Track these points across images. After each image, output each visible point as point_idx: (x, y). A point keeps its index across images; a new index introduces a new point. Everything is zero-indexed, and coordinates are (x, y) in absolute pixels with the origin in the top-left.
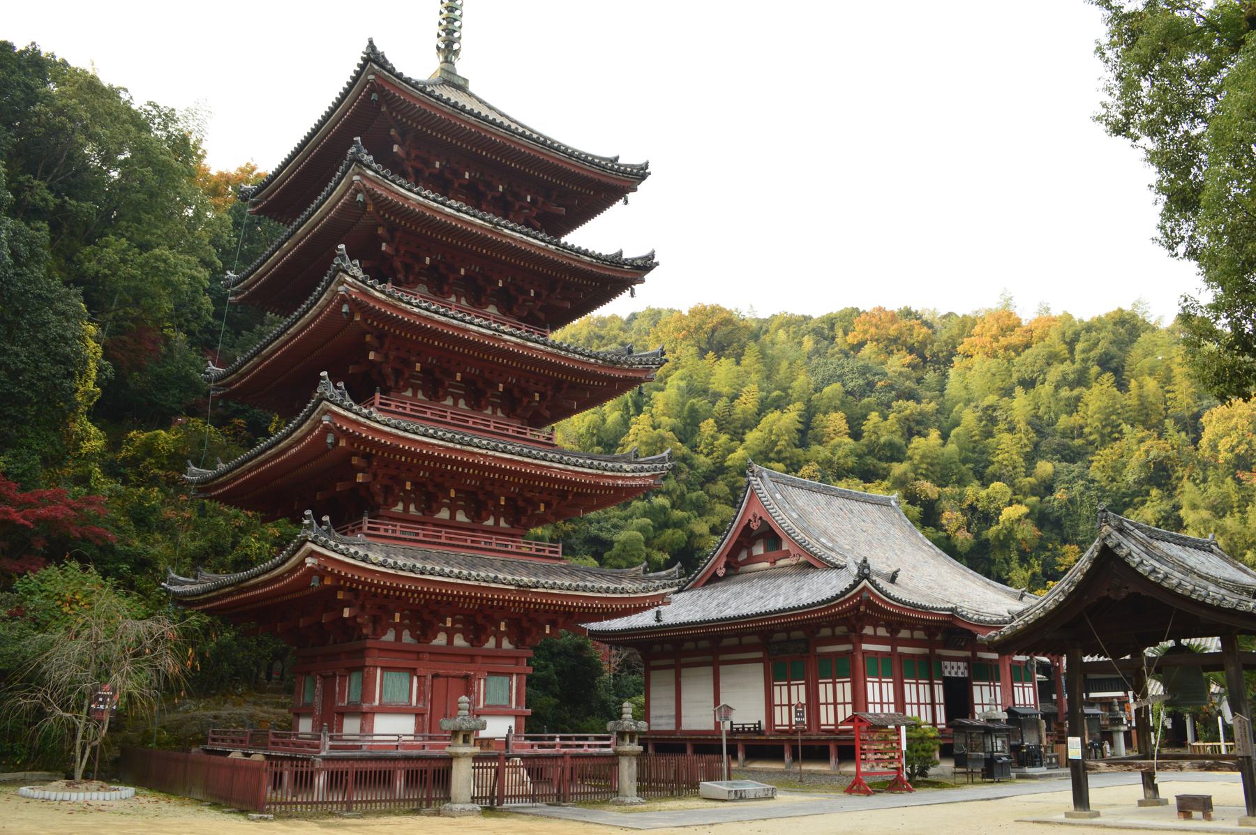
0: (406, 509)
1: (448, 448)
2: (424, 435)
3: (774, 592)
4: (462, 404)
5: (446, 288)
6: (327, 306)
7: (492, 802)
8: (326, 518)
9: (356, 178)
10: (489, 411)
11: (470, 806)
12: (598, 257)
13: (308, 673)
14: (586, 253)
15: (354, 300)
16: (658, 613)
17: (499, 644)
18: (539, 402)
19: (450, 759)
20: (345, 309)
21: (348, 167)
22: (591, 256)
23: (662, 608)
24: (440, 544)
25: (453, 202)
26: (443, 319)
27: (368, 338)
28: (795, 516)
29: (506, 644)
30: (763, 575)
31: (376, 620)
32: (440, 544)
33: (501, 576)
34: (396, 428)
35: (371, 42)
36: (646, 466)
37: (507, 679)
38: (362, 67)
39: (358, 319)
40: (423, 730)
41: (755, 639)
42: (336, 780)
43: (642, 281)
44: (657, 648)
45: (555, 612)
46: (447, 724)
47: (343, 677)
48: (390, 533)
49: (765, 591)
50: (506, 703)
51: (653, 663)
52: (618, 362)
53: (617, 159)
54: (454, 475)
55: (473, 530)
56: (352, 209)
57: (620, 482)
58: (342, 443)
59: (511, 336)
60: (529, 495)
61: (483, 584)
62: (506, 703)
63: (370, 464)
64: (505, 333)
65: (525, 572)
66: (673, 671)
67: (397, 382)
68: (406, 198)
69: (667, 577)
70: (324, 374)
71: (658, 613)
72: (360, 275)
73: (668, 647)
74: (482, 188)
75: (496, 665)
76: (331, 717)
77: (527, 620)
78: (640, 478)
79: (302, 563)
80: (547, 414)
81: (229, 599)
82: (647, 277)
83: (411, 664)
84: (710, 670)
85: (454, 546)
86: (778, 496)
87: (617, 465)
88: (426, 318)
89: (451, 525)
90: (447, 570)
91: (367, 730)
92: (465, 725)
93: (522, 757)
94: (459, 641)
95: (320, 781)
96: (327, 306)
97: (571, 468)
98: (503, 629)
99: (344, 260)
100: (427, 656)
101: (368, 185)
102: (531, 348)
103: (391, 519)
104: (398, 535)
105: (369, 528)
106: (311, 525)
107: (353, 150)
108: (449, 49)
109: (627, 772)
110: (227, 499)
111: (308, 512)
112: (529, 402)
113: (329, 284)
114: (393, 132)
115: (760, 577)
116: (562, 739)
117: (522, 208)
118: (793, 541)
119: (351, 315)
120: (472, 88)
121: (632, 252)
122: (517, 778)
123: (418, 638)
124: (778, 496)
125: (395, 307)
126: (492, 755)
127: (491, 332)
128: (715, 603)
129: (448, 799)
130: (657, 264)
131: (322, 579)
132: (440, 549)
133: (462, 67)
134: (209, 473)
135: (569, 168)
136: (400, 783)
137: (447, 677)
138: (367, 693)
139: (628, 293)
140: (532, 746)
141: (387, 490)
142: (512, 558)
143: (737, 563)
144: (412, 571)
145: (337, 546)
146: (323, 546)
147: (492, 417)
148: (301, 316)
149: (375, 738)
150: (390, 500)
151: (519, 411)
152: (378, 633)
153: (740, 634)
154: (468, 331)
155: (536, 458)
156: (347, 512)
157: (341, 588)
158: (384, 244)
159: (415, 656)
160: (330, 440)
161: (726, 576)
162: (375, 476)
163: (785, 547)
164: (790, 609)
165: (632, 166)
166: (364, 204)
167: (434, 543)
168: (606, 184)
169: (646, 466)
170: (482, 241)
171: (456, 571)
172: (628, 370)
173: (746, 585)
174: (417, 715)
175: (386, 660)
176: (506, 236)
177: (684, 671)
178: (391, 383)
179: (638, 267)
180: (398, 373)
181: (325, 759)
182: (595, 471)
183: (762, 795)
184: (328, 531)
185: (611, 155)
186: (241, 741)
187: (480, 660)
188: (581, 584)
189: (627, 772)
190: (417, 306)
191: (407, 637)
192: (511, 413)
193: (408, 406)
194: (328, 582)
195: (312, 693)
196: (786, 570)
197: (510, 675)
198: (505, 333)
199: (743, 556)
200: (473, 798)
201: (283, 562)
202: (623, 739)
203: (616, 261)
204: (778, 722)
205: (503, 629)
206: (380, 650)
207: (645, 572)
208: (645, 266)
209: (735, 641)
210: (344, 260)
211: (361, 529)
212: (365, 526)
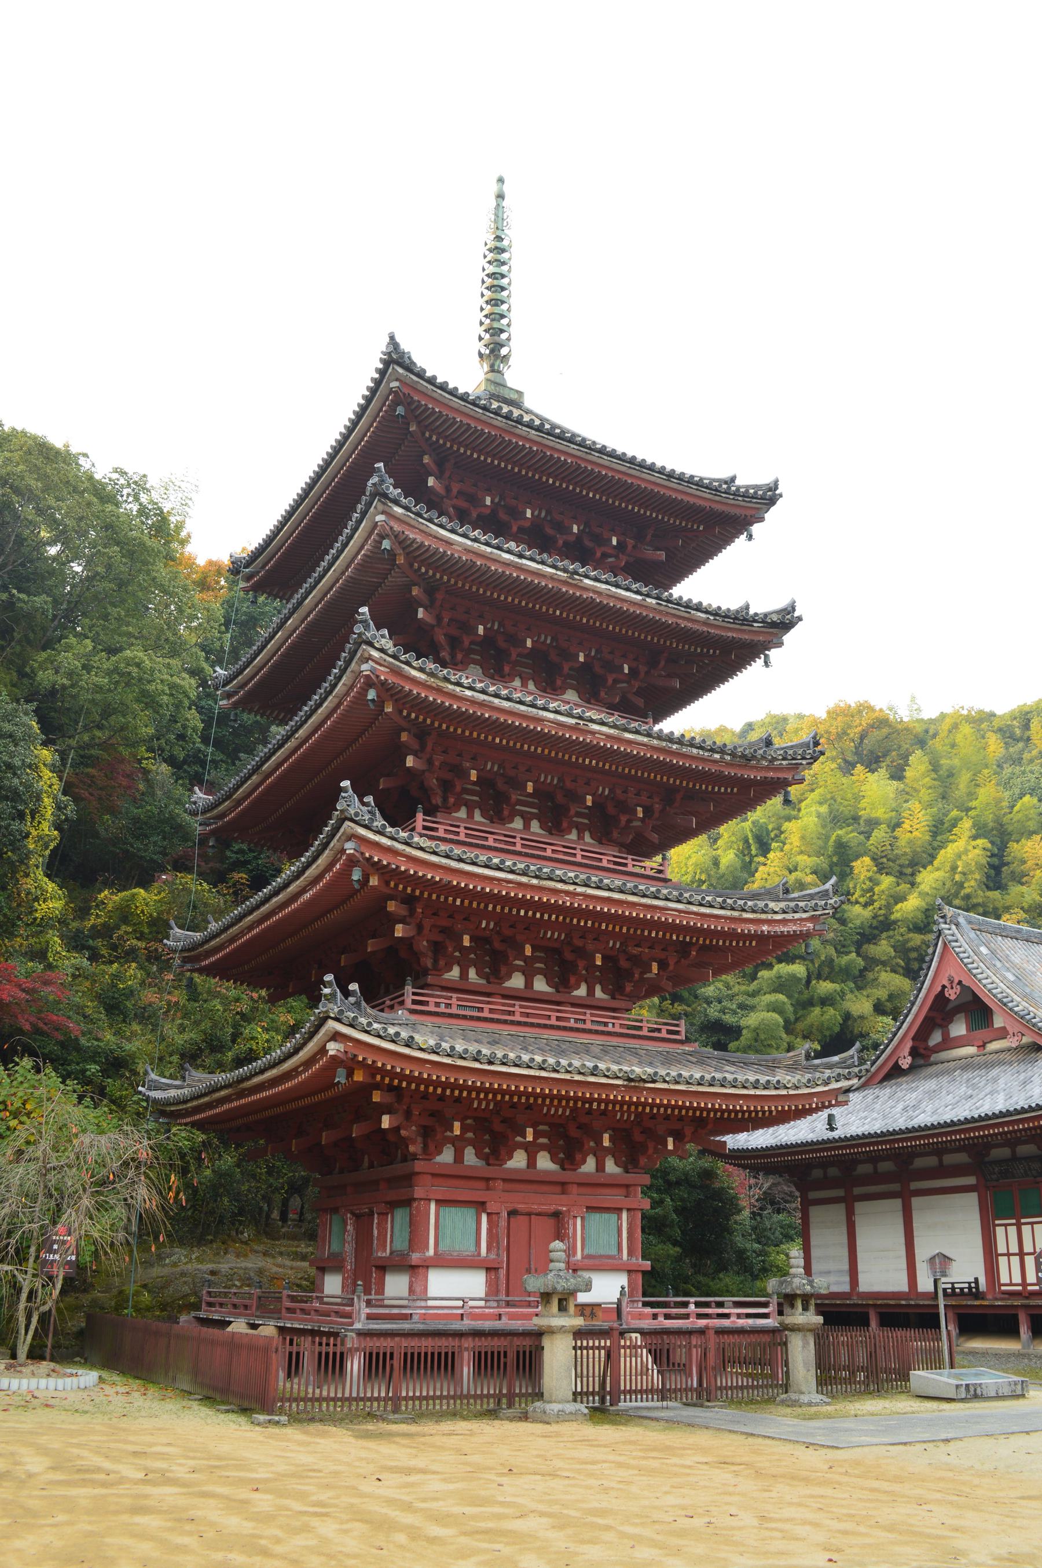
0: (464, 975)
1: (520, 884)
2: (486, 866)
3: (988, 1089)
4: (535, 826)
5: (507, 669)
6: (347, 694)
7: (603, 1400)
8: (354, 987)
9: (380, 518)
10: (573, 836)
11: (571, 1407)
12: (716, 613)
13: (335, 1210)
14: (698, 608)
15: (384, 684)
16: (831, 1118)
17: (600, 1167)
18: (642, 820)
19: (538, 1335)
20: (372, 694)
21: (369, 505)
22: (707, 612)
23: (835, 1111)
24: (512, 1023)
25: (512, 545)
26: (506, 704)
27: (404, 737)
28: (1012, 978)
29: (611, 1167)
30: (967, 1065)
31: (427, 1133)
32: (512, 1023)
33: (602, 1066)
34: (447, 857)
35: (392, 338)
36: (801, 904)
37: (614, 1217)
38: (382, 373)
39: (389, 709)
40: (497, 1292)
41: (961, 1158)
42: (377, 1365)
43: (780, 644)
44: (817, 1173)
45: (681, 1118)
46: (534, 1283)
47: (383, 1215)
48: (442, 1009)
49: (974, 1087)
50: (614, 1252)
51: (813, 1195)
52: (754, 757)
53: (733, 479)
54: (530, 925)
55: (558, 1003)
56: (378, 563)
57: (765, 928)
58: (374, 881)
59: (602, 726)
60: (635, 951)
61: (578, 1078)
62: (614, 1252)
63: (412, 912)
64: (592, 721)
65: (636, 1060)
66: (843, 1206)
67: (445, 799)
68: (449, 543)
69: (842, 1064)
70: (346, 784)
71: (831, 1118)
72: (388, 644)
73: (833, 1172)
74: (549, 531)
75: (598, 1197)
76: (368, 1272)
77: (637, 1130)
78: (794, 921)
79: (323, 1050)
80: (655, 837)
81: (226, 1107)
82: (787, 638)
83: (478, 1196)
84: (897, 1203)
85: (532, 1025)
86: (984, 950)
87: (761, 904)
88: (482, 704)
89: (527, 996)
90: (526, 1058)
91: (417, 1292)
92: (562, 1285)
93: (642, 1332)
94: (544, 1162)
95: (355, 1365)
96: (347, 694)
97: (695, 909)
98: (606, 1143)
99: (367, 627)
100: (499, 1184)
101: (397, 527)
102: (630, 742)
103: (444, 988)
104: (454, 1010)
105: (414, 1002)
106: (333, 995)
107: (375, 479)
108: (495, 352)
109: (801, 1354)
110: (222, 970)
111: (329, 977)
112: (629, 821)
113: (348, 663)
114: (426, 460)
115: (964, 1068)
116: (698, 1305)
117: (605, 555)
118: (1011, 1013)
119: (380, 703)
120: (528, 403)
121: (764, 603)
122: (636, 1364)
123: (486, 1159)
124: (984, 950)
125: (439, 690)
126: (599, 1330)
127: (573, 721)
128: (900, 1106)
129: (539, 1395)
130: (800, 619)
131: (350, 1074)
132: (513, 1030)
133: (513, 377)
134: (198, 936)
135: (668, 493)
136: (466, 1371)
137: (529, 1214)
138: (416, 1236)
139: (760, 662)
140: (655, 1316)
141: (437, 948)
142: (615, 1041)
143: (927, 1048)
144: (476, 1060)
145: (369, 1024)
146: (351, 1026)
147: (580, 843)
148: (313, 711)
149: (430, 1303)
150: (442, 963)
151: (615, 835)
152: (431, 1150)
153: (939, 1151)
154: (540, 720)
155: (644, 896)
156: (382, 981)
157: (377, 1086)
158: (421, 610)
159: (482, 1184)
160: (356, 875)
161: (913, 1068)
162: (420, 927)
163: (998, 1022)
164: (1017, 1112)
165: (757, 487)
166: (392, 554)
167: (505, 1022)
168: (720, 515)
169: (801, 904)
170: (555, 598)
171: (539, 1059)
172: (767, 769)
173: (945, 1079)
174: (488, 1270)
175: (442, 1190)
176: (586, 589)
177: (860, 1207)
178: (438, 800)
179: (773, 625)
180: (446, 786)
181: (361, 1334)
182: (728, 913)
183: (1006, 1391)
184: (357, 1004)
185: (724, 474)
186: (246, 1307)
187: (574, 1189)
188: (718, 1076)
189: (801, 1354)
190: (469, 688)
191: (470, 1157)
192: (603, 836)
193: (462, 830)
194: (359, 1077)
195: (341, 1238)
196: (1002, 1056)
197: (619, 1210)
198: (592, 721)
199: (936, 1038)
200: (575, 1394)
201: (297, 1050)
202: (792, 1306)
203: (741, 618)
204: (1004, 1278)
205: (606, 1143)
206: (433, 1175)
207: (808, 1057)
208: (782, 622)
209: (932, 1161)
210: (367, 627)
211: (402, 1003)
212: (409, 998)
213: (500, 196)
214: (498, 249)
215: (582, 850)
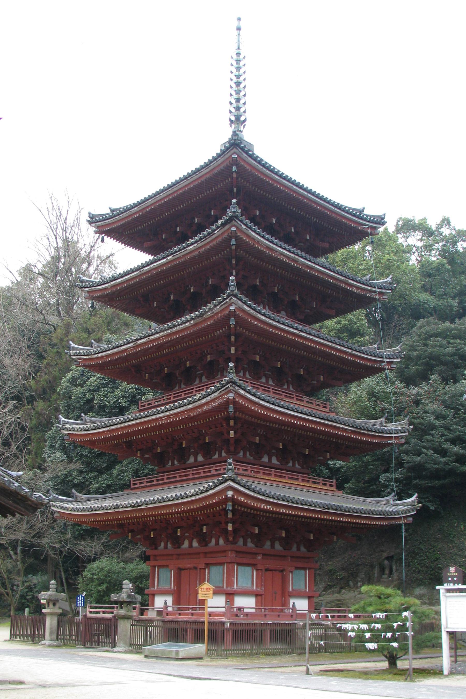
37: (303, 572)
133: (248, 135)
215: (296, 396)
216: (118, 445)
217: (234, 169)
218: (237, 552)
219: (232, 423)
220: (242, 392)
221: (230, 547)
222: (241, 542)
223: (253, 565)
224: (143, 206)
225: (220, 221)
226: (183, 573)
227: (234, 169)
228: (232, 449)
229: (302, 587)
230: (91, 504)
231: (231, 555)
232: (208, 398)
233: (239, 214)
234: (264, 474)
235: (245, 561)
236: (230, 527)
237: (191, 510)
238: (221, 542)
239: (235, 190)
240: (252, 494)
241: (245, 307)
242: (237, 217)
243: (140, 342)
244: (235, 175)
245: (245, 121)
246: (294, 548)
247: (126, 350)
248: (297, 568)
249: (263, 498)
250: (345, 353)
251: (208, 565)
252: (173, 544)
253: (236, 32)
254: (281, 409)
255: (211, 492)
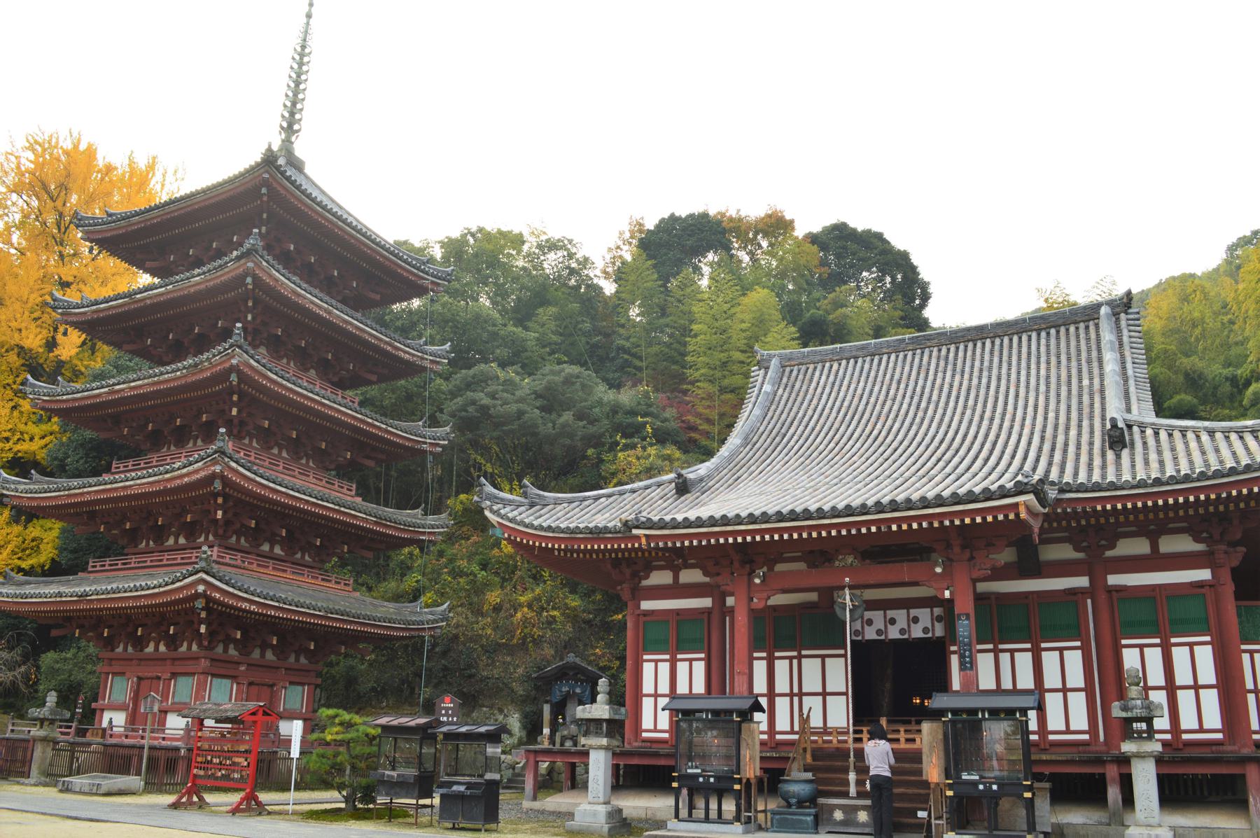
37: (300, 688)
108: (290, 128)
120: (307, 170)
133: (300, 150)
213: (309, 16)
214: (302, 54)
216: (77, 514)
217: (264, 190)
218: (212, 660)
219: (220, 500)
220: (233, 465)
221: (203, 653)
222: (220, 649)
223: (233, 678)
224: (147, 216)
225: (235, 253)
226: (143, 683)
227: (264, 190)
228: (221, 532)
229: (298, 706)
230: (28, 590)
231: (204, 663)
232: (191, 468)
233: (260, 249)
234: (259, 565)
235: (222, 672)
236: (203, 629)
237: (152, 606)
238: (195, 647)
239: (265, 216)
240: (231, 590)
241: (252, 361)
242: (256, 251)
243: (117, 387)
244: (265, 199)
245: (298, 131)
246: (292, 659)
247: (99, 395)
248: (291, 683)
249: (245, 595)
250: (379, 428)
251: (174, 675)
252: (134, 647)
253: (305, 20)
254: (284, 490)
255: (178, 584)
